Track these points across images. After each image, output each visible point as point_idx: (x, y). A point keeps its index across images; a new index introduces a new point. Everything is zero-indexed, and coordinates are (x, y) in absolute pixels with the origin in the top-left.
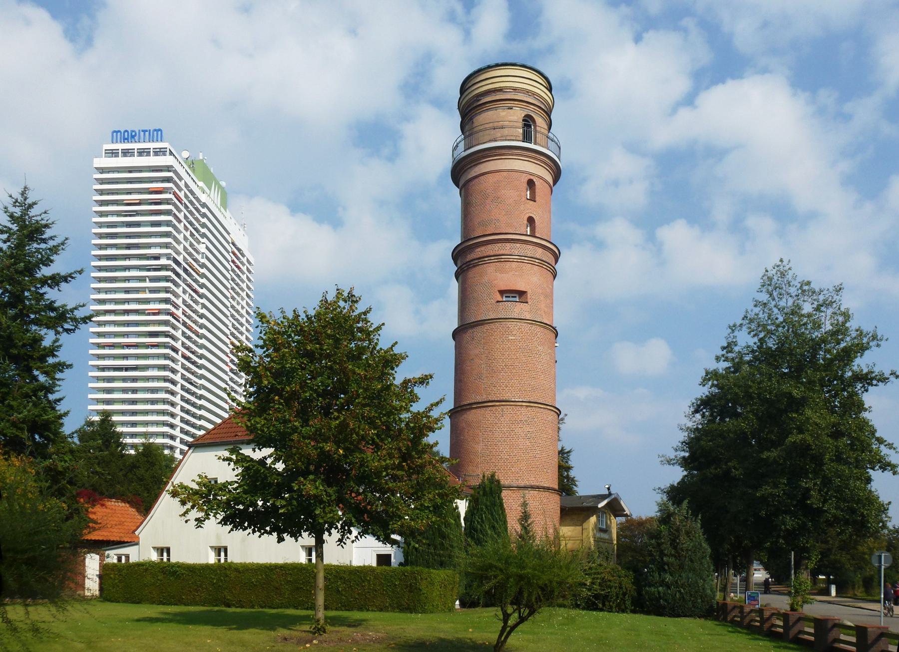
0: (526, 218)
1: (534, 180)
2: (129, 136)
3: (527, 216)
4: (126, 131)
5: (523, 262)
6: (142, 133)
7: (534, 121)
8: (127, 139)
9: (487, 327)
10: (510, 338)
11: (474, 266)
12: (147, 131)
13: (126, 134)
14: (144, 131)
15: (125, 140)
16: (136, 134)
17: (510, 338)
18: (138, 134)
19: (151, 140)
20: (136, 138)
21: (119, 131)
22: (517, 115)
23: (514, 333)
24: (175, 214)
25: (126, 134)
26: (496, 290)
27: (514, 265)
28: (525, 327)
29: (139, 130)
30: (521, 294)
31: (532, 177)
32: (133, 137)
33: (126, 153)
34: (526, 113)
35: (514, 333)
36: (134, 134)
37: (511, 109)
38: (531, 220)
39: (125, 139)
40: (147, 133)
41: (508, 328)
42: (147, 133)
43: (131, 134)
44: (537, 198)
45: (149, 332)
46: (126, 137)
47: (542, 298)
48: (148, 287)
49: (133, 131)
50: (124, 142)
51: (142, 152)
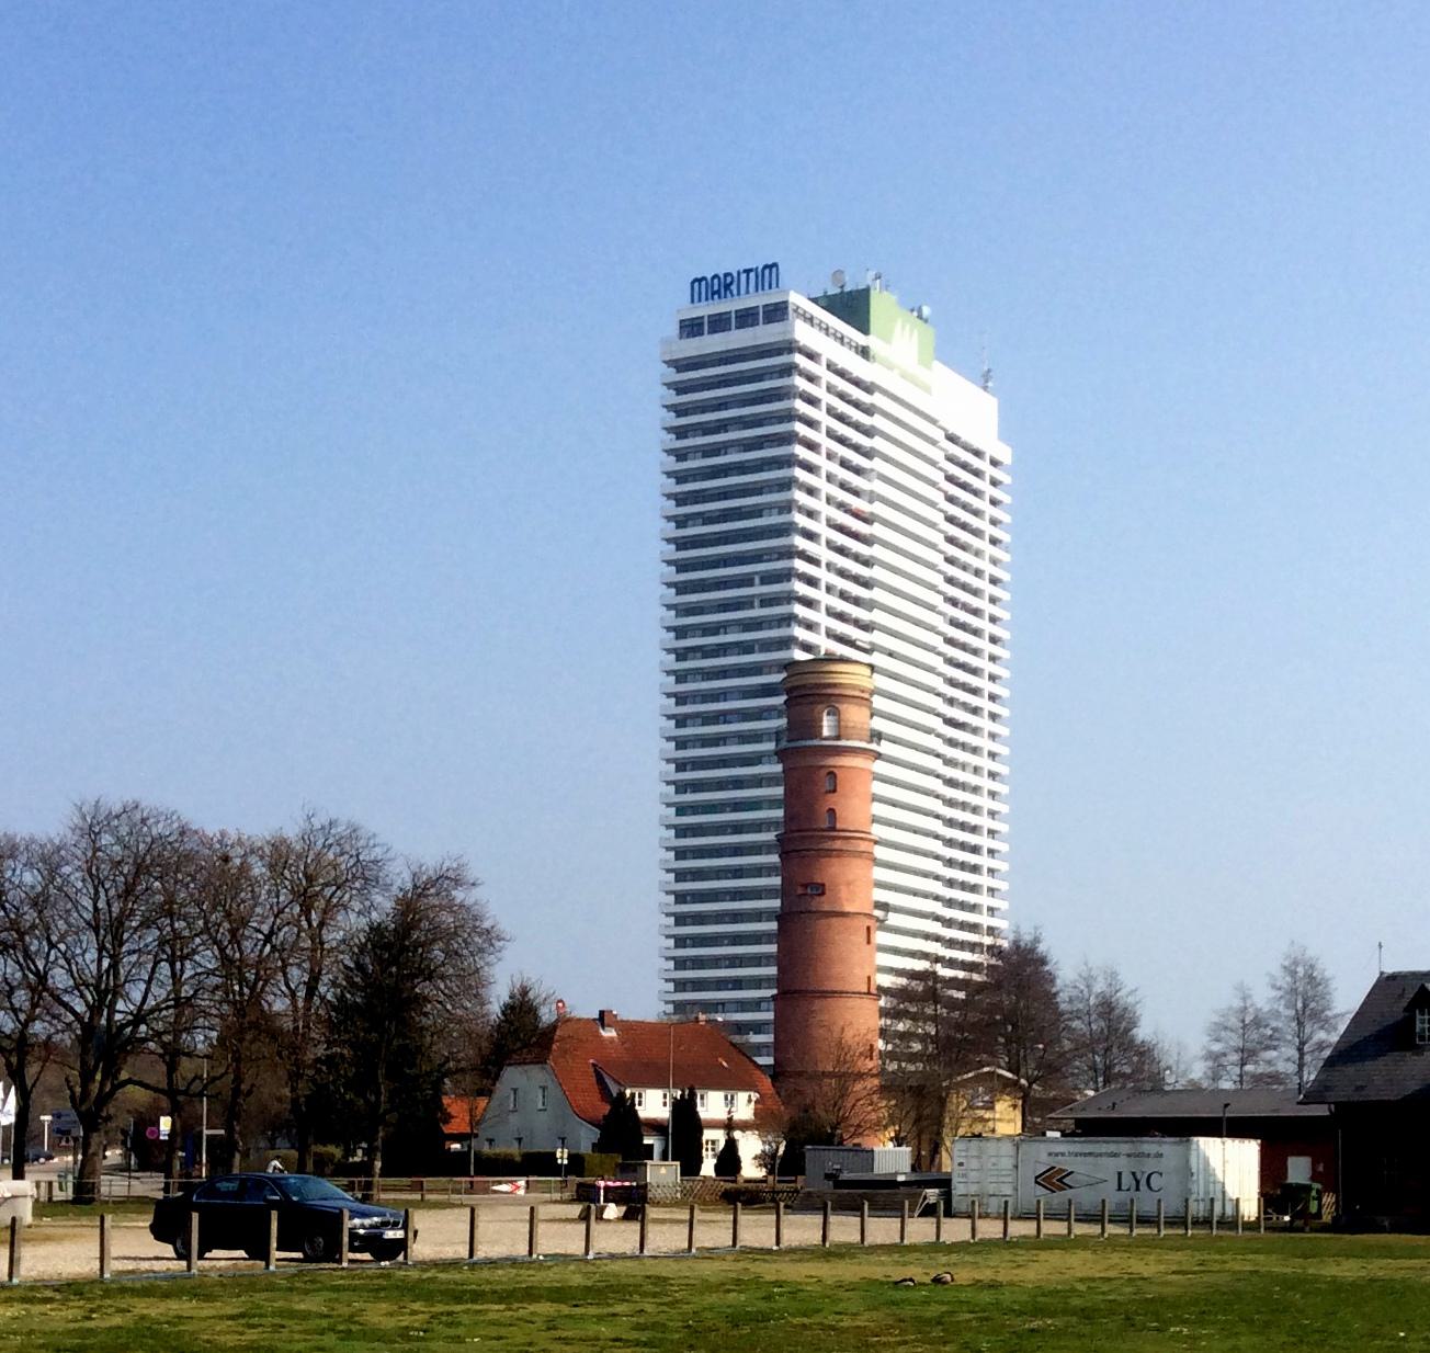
6: (743, 276)
8: (718, 292)
12: (751, 270)
13: (716, 281)
14: (748, 271)
15: (715, 294)
16: (732, 278)
18: (736, 279)
20: (734, 287)
21: (704, 278)
25: (716, 281)
29: (739, 273)
31: (832, 769)
32: (727, 287)
36: (729, 280)
38: (832, 811)
39: (713, 294)
40: (752, 275)
42: (752, 275)
43: (725, 280)
46: (716, 288)
49: (726, 275)
50: (713, 299)
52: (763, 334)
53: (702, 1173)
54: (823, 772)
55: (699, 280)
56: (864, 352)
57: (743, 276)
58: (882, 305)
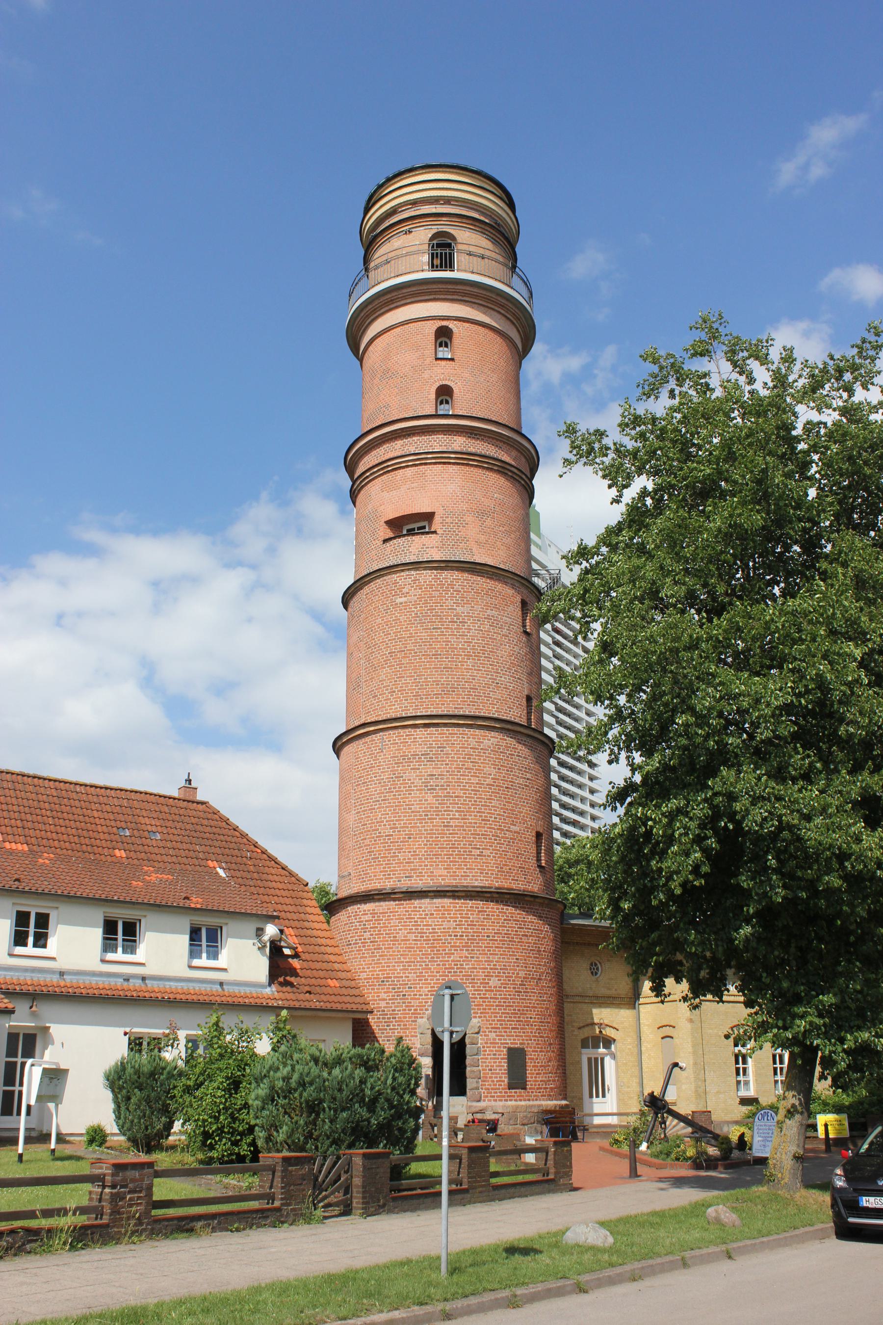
3: (437, 385)
5: (426, 464)
7: (453, 238)
9: (366, 590)
10: (399, 600)
11: (359, 491)
17: (399, 600)
22: (422, 235)
23: (405, 590)
26: (382, 523)
27: (409, 472)
28: (427, 576)
30: (429, 517)
31: (445, 323)
34: (434, 230)
35: (405, 590)
37: (410, 232)
38: (444, 393)
41: (396, 583)
47: (469, 518)
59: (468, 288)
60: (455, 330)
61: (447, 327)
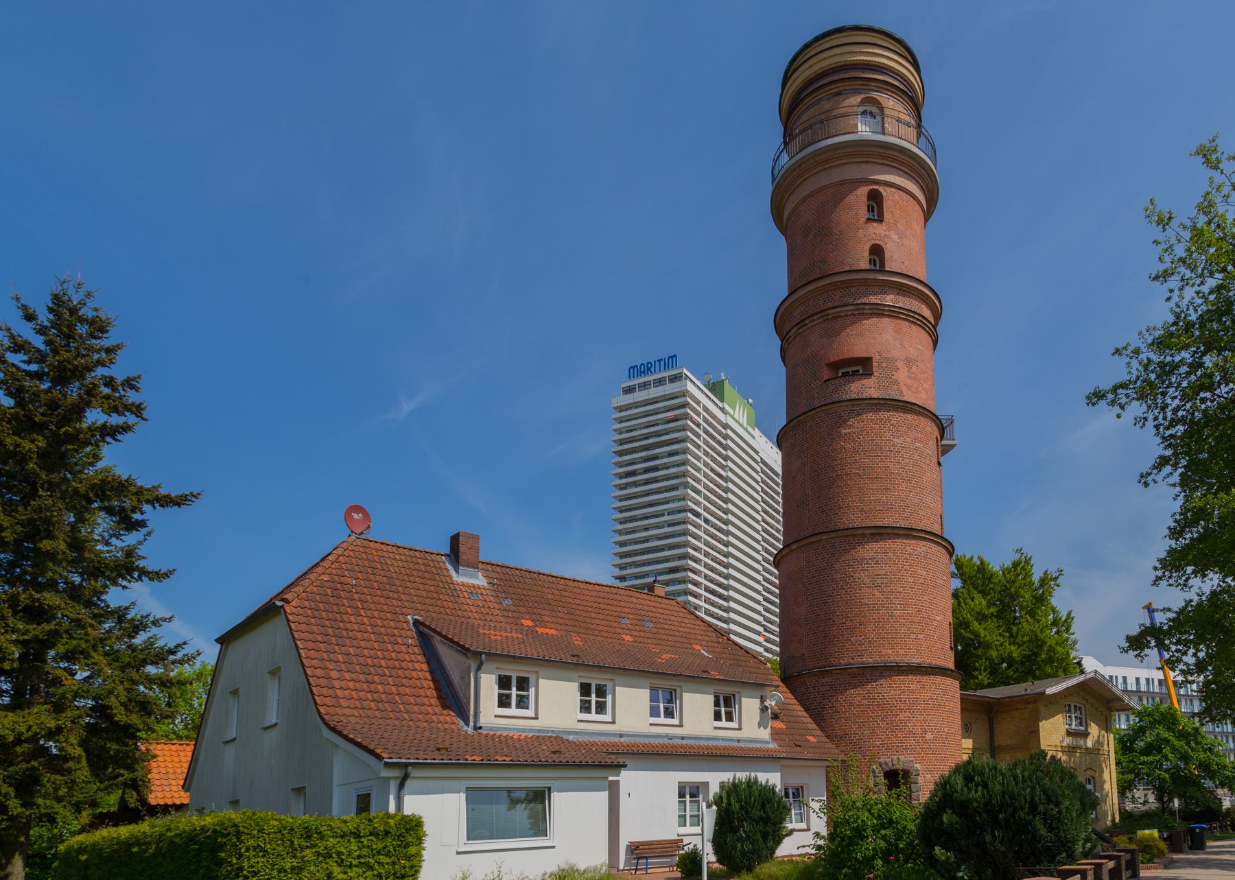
0: (867, 248)
1: (881, 189)
2: (647, 369)
3: (870, 243)
4: (643, 364)
6: (657, 363)
8: (644, 372)
14: (660, 361)
19: (667, 367)
20: (652, 369)
21: (636, 366)
24: (692, 439)
31: (876, 187)
32: (649, 369)
33: (645, 386)
39: (641, 373)
40: (662, 363)
42: (662, 363)
44: (887, 216)
45: (669, 568)
48: (666, 521)
49: (648, 363)
51: (660, 382)
52: (669, 388)
53: (963, 740)
54: (863, 191)
55: (633, 367)
56: (722, 409)
57: (657, 363)
58: (728, 388)
59: (897, 154)
60: (884, 194)
61: (877, 190)
